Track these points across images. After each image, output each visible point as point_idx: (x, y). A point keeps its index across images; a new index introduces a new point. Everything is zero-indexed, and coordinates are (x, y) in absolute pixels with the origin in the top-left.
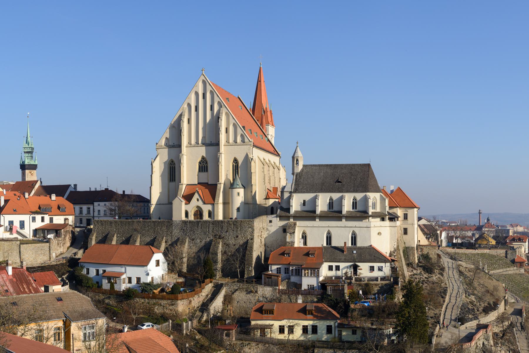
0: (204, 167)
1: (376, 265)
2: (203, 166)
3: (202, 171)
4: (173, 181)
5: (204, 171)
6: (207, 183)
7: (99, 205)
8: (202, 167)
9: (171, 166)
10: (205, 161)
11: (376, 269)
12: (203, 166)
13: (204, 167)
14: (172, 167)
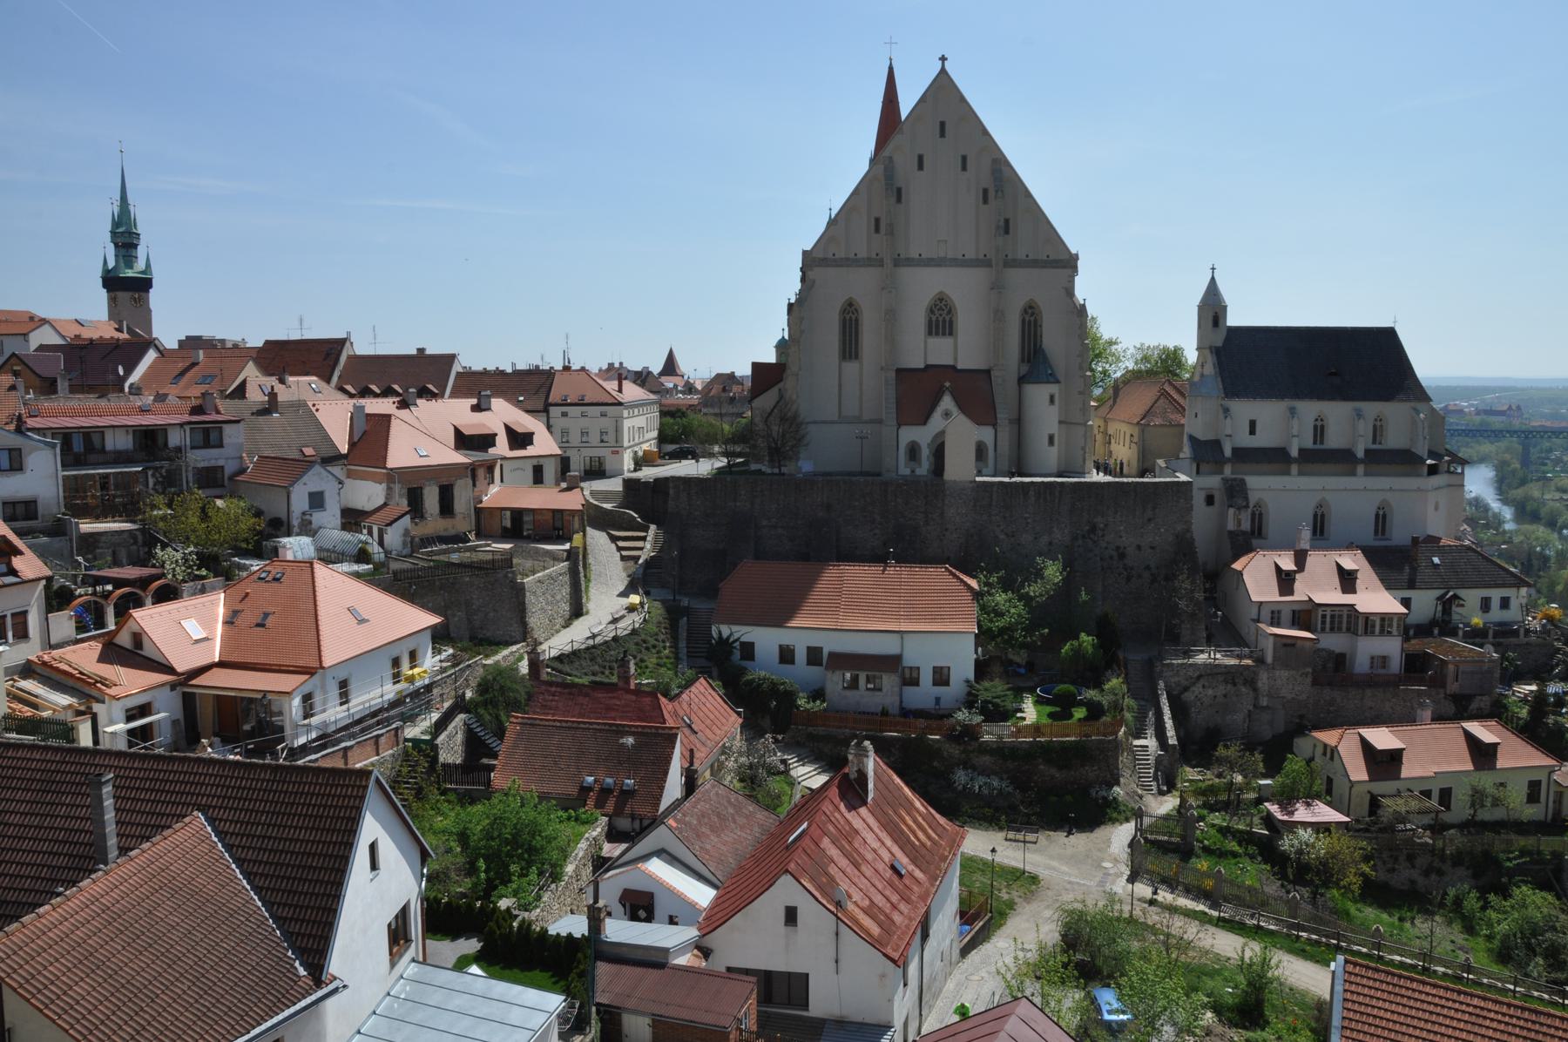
0: (944, 321)
1: (1496, 595)
2: (941, 319)
3: (937, 334)
4: (850, 357)
5: (944, 334)
6: (953, 368)
7: (564, 414)
8: (937, 320)
9: (848, 317)
10: (946, 305)
11: (1495, 603)
12: (941, 319)
13: (944, 321)
14: (851, 319)
